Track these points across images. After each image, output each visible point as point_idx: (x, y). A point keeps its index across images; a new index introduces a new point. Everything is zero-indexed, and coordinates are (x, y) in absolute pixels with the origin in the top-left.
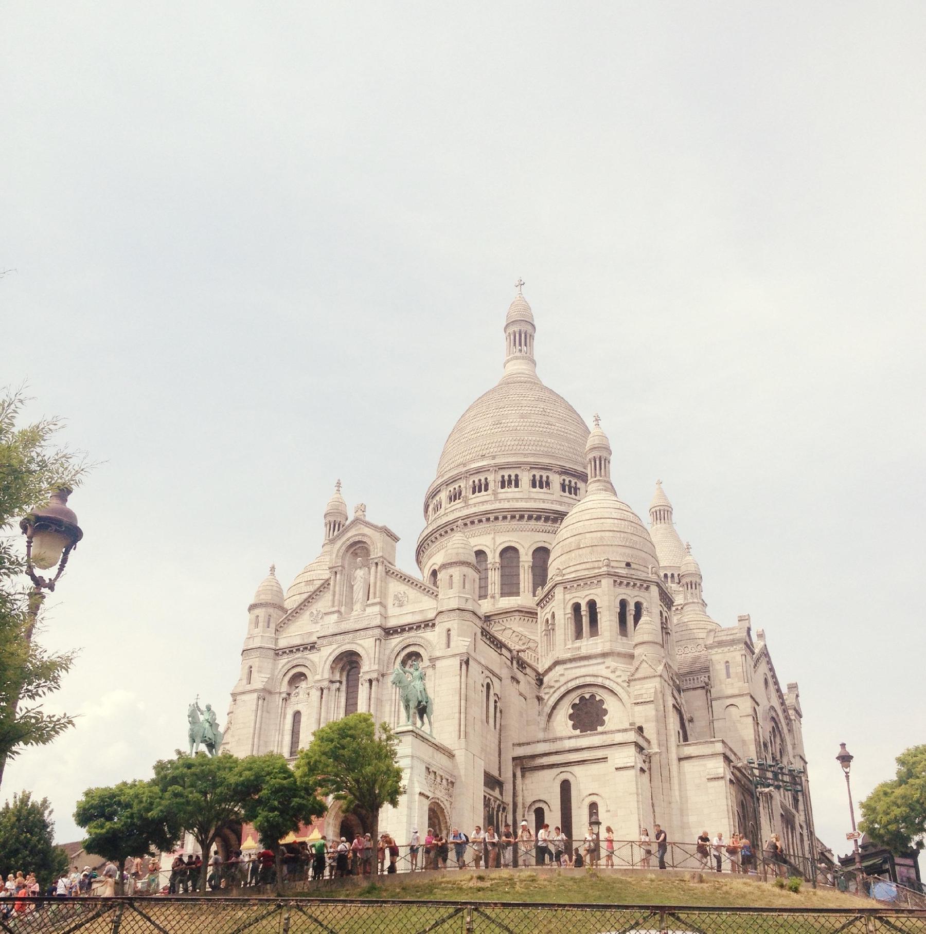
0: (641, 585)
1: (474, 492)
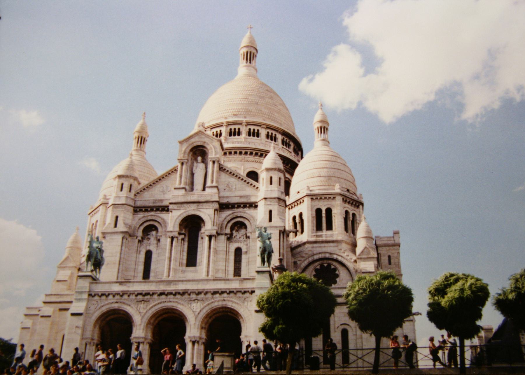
0: (356, 204)
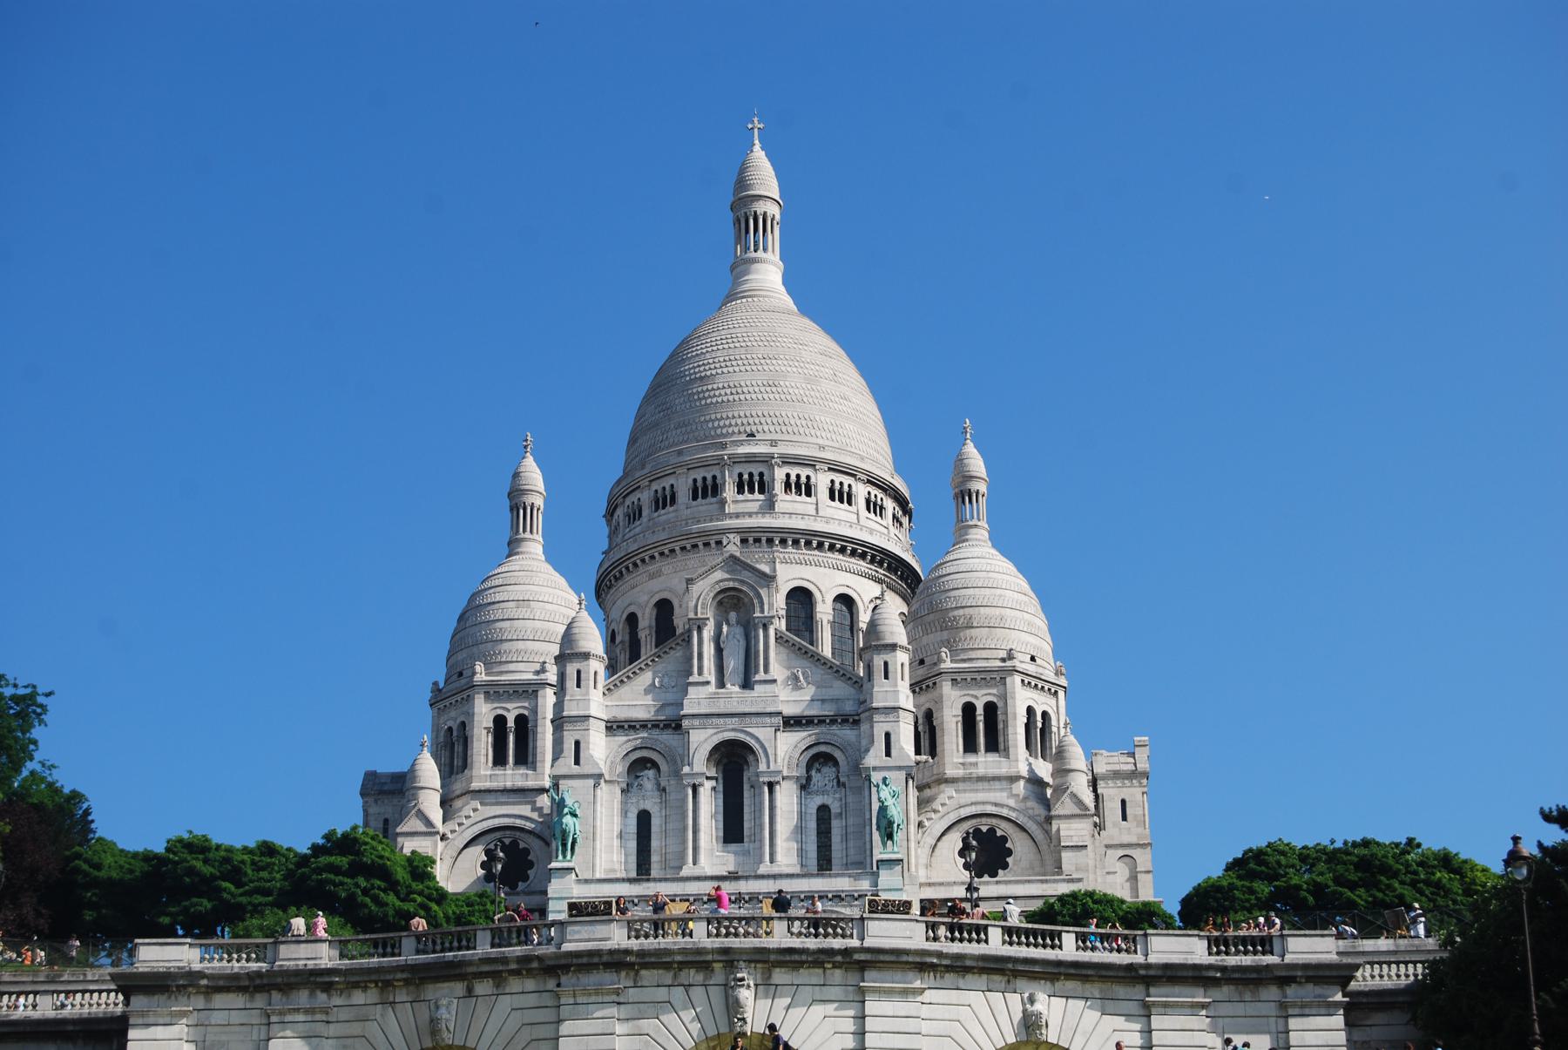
0: (1049, 689)
1: (740, 491)
